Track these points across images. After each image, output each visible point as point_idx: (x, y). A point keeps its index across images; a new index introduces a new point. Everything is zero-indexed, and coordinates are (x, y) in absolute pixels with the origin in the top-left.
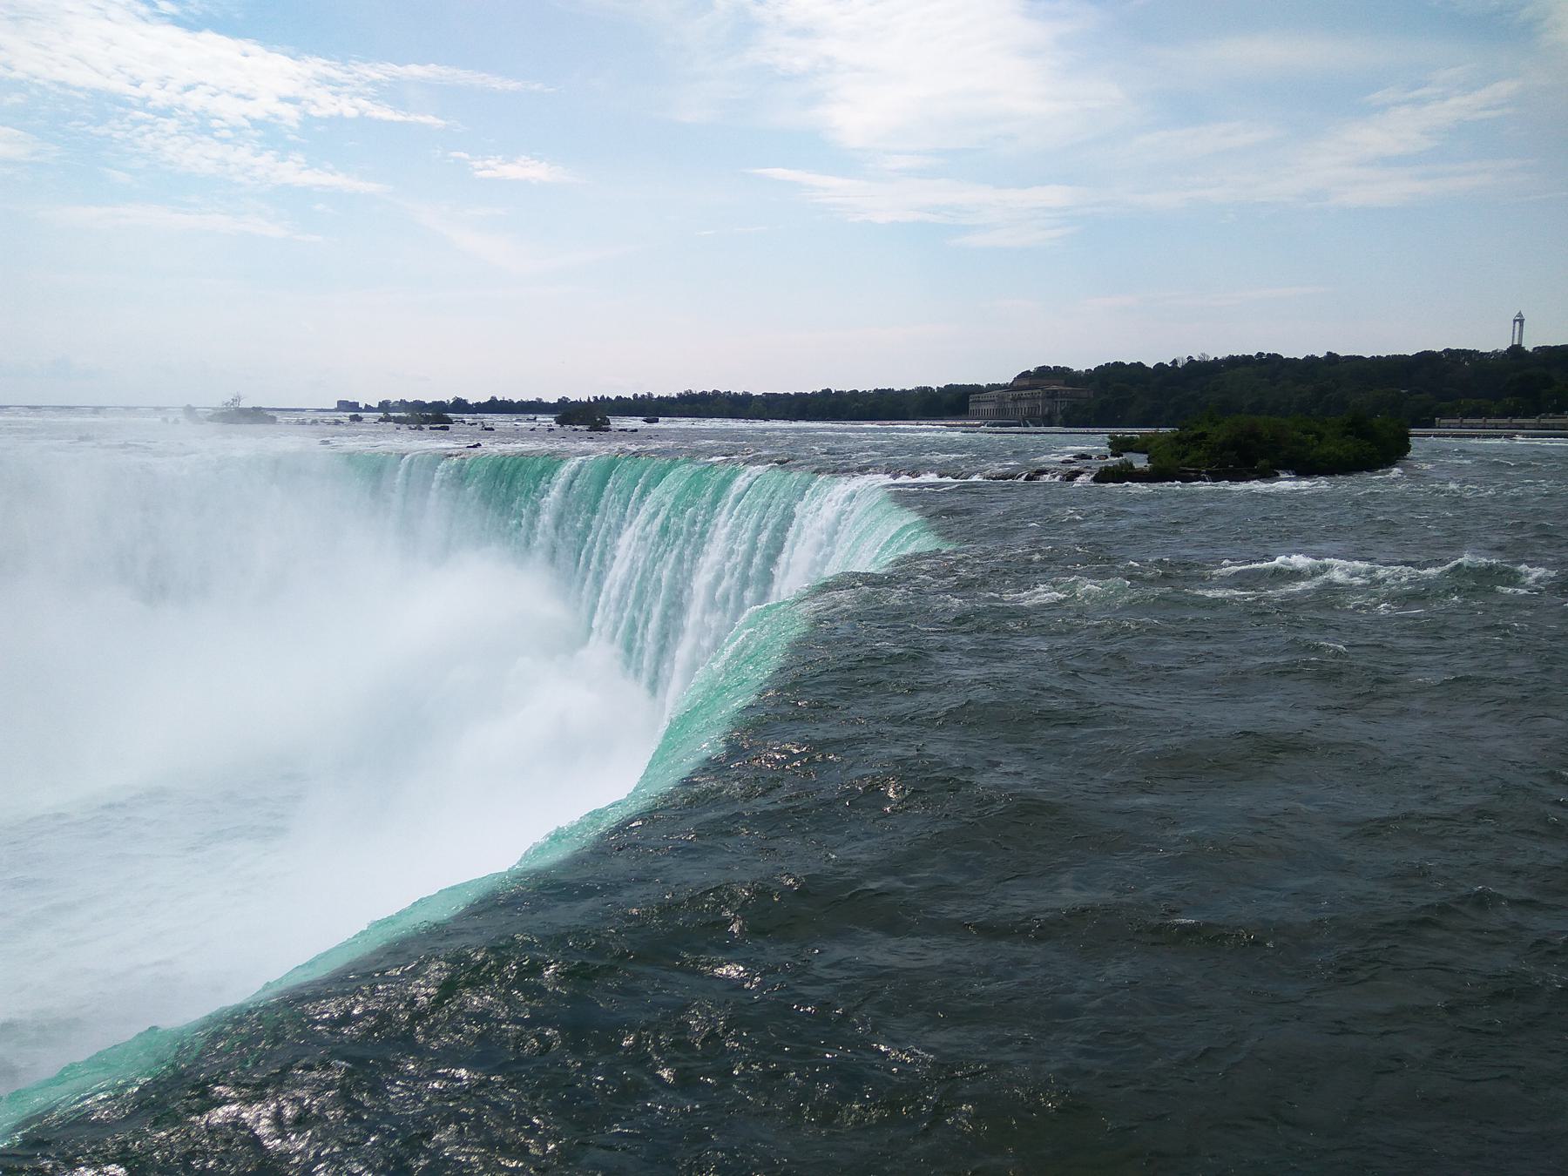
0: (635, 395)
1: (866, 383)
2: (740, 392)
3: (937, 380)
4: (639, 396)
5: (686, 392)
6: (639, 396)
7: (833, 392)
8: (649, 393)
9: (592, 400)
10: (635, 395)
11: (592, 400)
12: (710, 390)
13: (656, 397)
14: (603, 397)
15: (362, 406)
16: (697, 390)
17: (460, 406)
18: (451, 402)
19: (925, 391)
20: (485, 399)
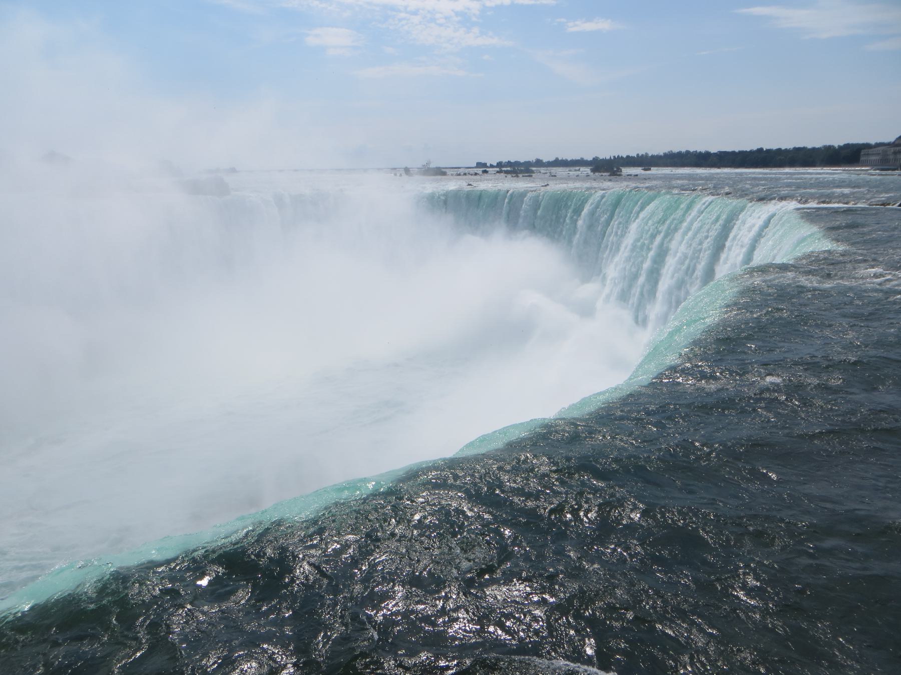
0: (638, 155)
1: (787, 144)
2: (703, 151)
3: (838, 140)
4: (640, 155)
5: (669, 152)
6: (640, 155)
7: (765, 150)
8: (646, 153)
9: (612, 158)
10: (638, 155)
11: (612, 158)
12: (683, 150)
13: (650, 155)
14: (618, 156)
16: (676, 150)
17: (539, 163)
18: (534, 161)
19: (829, 148)
20: (552, 159)
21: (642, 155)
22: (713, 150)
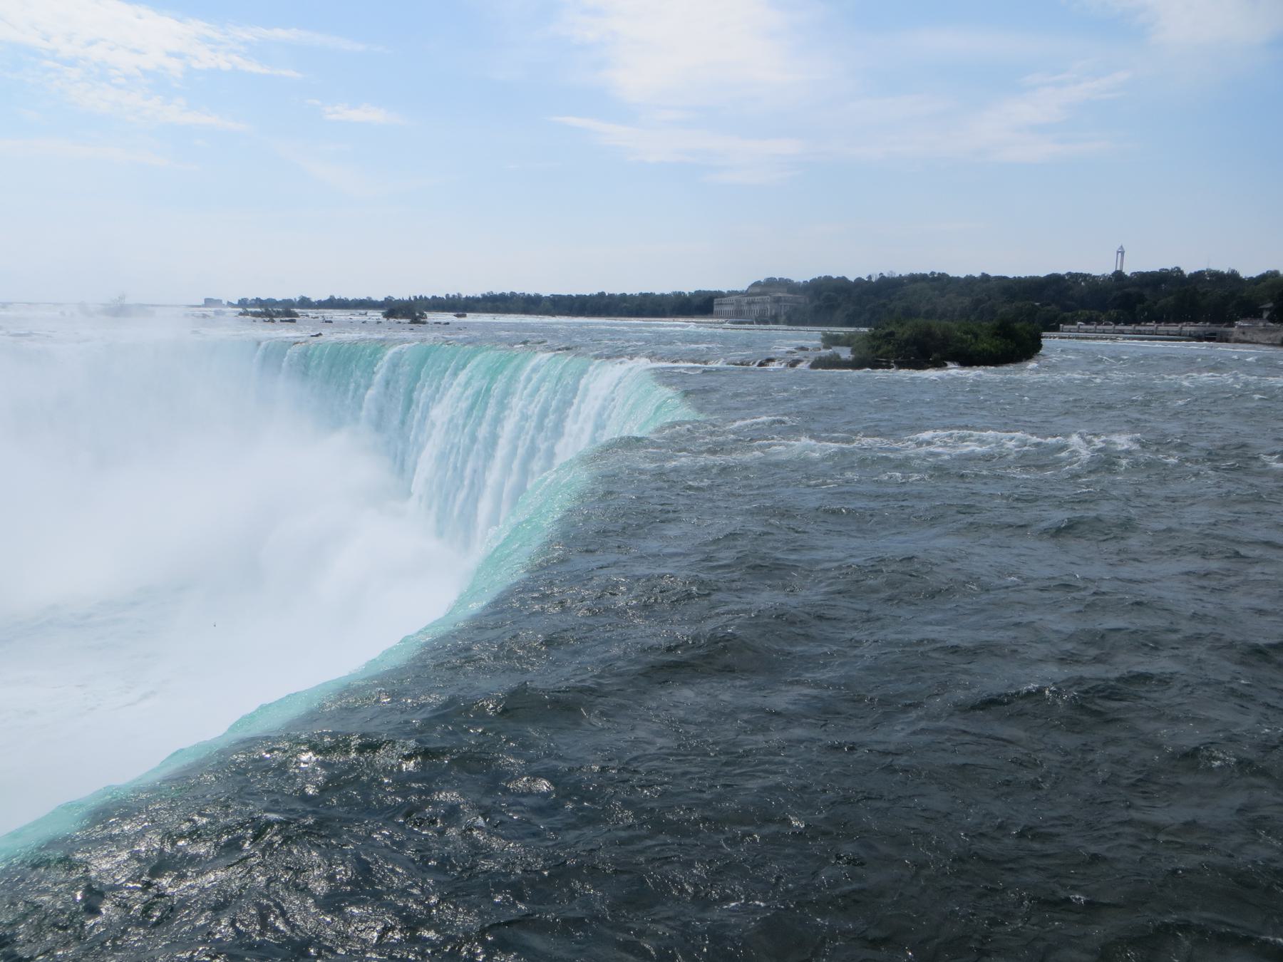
0: (447, 295)
1: (633, 287)
2: (532, 293)
3: (688, 288)
4: (451, 296)
6: (451, 296)
9: (412, 299)
10: (447, 295)
11: (412, 299)
13: (464, 296)
14: (421, 297)
15: (225, 302)
16: (497, 291)
17: (305, 303)
18: (298, 299)
19: (679, 296)
20: (324, 297)
21: (454, 296)
22: (546, 292)
